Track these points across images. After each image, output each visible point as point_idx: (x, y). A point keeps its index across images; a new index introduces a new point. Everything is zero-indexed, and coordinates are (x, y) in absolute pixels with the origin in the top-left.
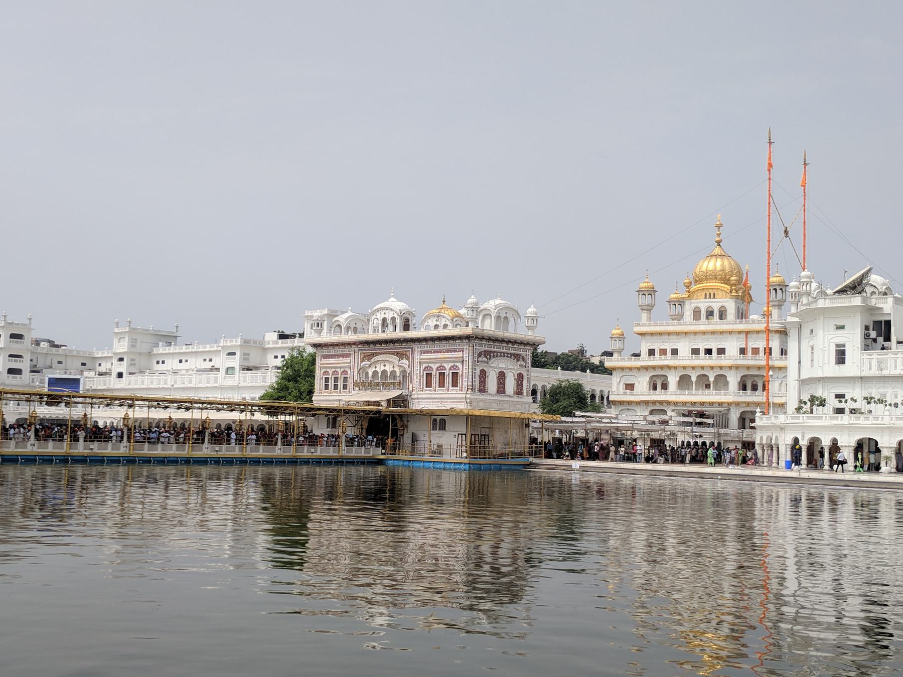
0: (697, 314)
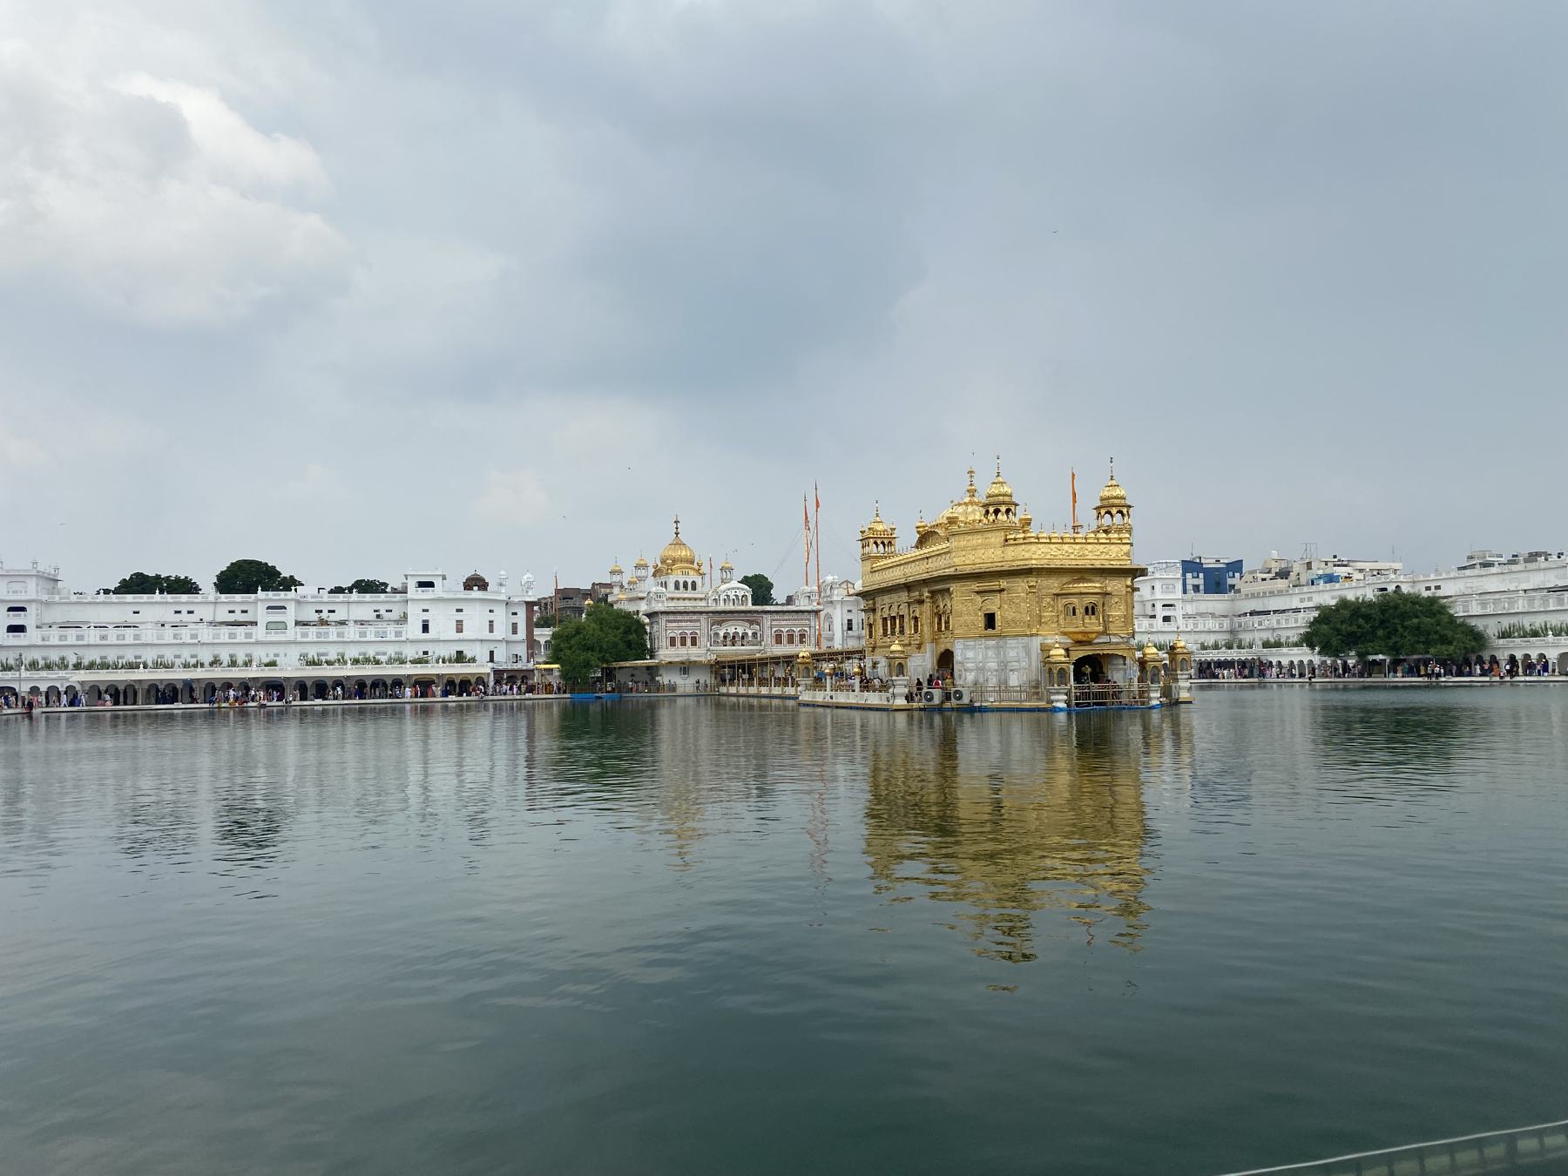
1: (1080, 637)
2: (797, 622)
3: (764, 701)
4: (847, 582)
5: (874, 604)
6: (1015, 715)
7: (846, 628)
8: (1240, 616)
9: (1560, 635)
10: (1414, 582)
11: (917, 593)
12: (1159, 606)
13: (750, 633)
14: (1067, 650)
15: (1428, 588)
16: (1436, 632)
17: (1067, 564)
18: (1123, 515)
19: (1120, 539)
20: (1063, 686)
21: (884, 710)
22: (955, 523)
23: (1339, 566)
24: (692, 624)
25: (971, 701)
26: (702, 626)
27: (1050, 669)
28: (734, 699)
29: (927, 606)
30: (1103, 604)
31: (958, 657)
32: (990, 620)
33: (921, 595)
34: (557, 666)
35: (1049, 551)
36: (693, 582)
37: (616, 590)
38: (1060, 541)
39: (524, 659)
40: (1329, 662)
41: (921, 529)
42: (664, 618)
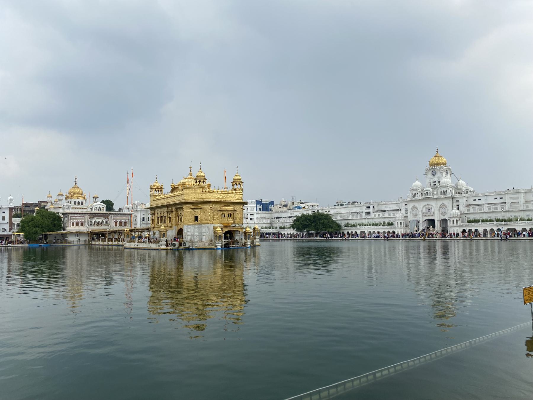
0: (75, 203)
1: (226, 225)
2: (123, 218)
3: (110, 247)
4: (143, 204)
5: (154, 212)
6: (204, 251)
7: (142, 220)
8: (273, 219)
9: (360, 226)
10: (322, 209)
11: (171, 209)
12: (249, 215)
13: (105, 222)
14: (222, 229)
15: (326, 211)
16: (328, 225)
17: (223, 200)
18: (240, 185)
19: (239, 193)
20: (220, 241)
21: (157, 250)
22: (185, 184)
23: (302, 204)
24: (82, 218)
25: (189, 246)
26: (86, 219)
27: (216, 235)
28: (97, 246)
29: (174, 213)
30: (234, 214)
31: (185, 231)
32: (196, 218)
33: (172, 209)
34: (22, 233)
35: (217, 196)
36: (82, 202)
37: (49, 204)
38: (220, 192)
39: (8, 230)
40: (298, 233)
41: (173, 186)
42: (70, 215)
